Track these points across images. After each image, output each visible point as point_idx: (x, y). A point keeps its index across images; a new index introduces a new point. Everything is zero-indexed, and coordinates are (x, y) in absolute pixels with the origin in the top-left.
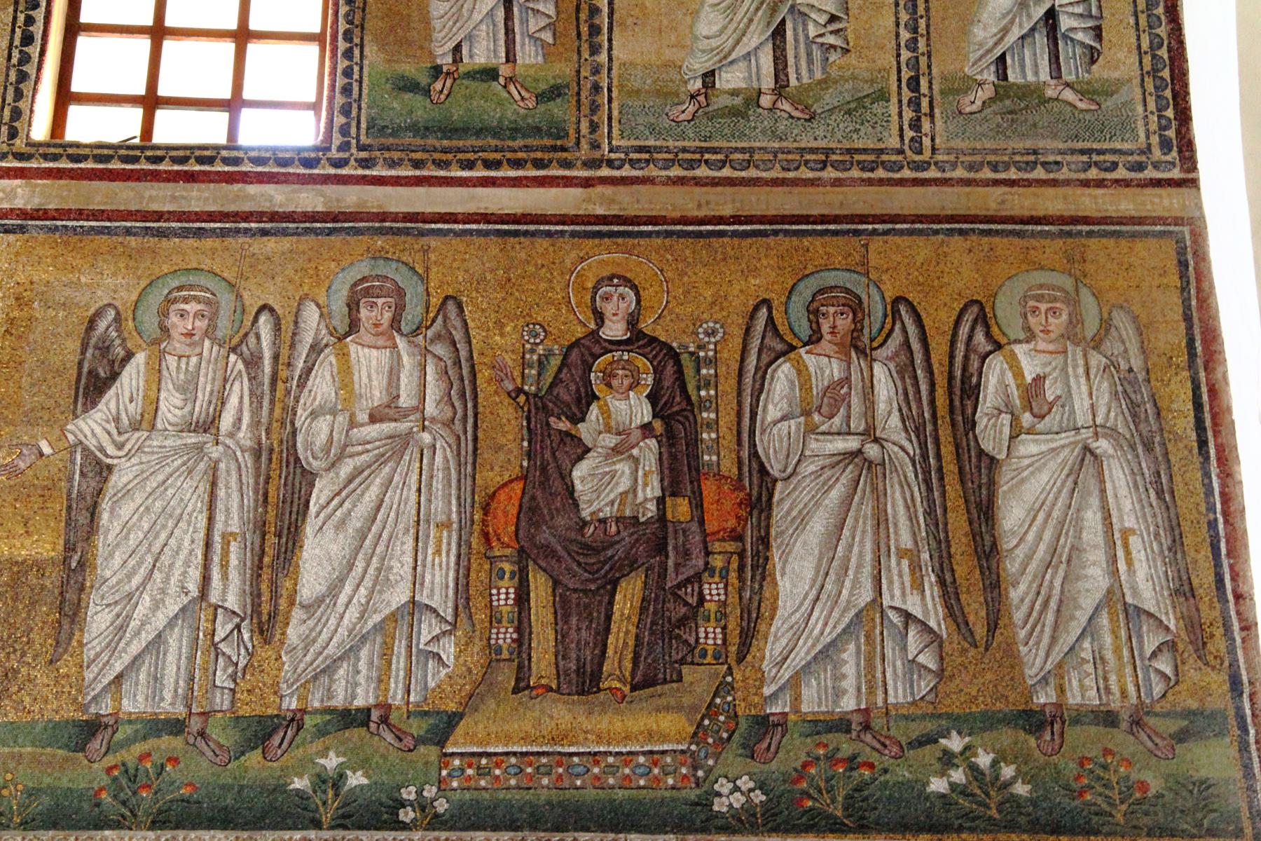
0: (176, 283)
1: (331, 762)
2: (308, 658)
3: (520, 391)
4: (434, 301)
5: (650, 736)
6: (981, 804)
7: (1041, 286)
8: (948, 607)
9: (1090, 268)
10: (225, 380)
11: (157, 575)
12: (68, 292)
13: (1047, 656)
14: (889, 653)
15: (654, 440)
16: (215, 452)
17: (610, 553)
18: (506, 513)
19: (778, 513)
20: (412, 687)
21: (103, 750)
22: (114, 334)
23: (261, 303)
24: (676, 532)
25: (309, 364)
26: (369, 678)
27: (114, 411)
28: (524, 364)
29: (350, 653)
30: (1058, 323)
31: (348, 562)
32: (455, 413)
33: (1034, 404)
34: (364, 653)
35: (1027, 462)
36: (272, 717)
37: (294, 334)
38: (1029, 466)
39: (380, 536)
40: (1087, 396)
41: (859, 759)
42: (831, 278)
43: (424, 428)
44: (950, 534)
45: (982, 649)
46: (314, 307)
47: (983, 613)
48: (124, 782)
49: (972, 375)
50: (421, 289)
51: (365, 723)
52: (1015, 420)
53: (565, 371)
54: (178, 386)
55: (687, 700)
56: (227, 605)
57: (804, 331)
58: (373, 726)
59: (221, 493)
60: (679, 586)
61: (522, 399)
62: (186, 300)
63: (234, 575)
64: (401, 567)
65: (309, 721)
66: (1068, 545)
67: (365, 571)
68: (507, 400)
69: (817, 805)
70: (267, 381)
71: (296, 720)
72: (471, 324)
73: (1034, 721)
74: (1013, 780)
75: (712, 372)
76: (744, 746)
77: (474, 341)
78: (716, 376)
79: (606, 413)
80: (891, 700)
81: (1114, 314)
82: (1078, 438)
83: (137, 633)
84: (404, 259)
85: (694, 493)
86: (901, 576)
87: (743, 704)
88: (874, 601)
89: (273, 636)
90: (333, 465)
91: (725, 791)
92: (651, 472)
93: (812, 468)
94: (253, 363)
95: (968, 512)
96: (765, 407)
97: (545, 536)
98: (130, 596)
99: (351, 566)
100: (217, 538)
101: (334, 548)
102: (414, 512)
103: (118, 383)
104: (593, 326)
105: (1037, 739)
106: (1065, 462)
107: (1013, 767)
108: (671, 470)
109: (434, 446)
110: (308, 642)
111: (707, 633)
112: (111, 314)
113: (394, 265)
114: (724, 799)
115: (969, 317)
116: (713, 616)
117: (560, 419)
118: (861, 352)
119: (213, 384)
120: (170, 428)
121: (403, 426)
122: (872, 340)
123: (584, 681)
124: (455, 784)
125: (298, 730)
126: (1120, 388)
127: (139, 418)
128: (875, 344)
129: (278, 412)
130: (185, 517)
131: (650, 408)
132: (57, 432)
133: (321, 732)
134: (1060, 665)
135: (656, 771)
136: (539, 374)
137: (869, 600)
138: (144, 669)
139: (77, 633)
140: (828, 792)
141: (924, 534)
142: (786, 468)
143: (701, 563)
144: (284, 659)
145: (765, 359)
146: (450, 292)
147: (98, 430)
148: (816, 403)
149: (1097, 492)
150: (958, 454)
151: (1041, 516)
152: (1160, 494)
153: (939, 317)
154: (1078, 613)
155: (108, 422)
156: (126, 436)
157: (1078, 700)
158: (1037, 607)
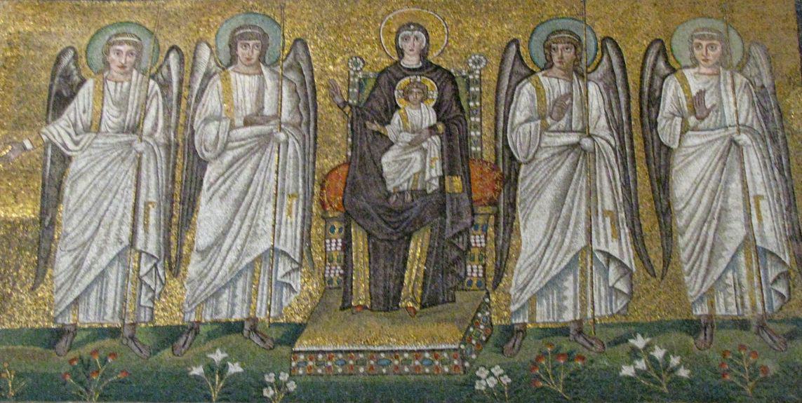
0: (114, 31)
1: (218, 356)
2: (202, 287)
3: (345, 103)
4: (287, 42)
6: (656, 383)
7: (703, 29)
8: (637, 251)
9: (737, 16)
10: (147, 98)
11: (102, 231)
12: (42, 39)
13: (704, 281)
14: (596, 281)
15: (438, 137)
16: (140, 147)
17: (406, 215)
19: (521, 187)
20: (272, 306)
21: (67, 348)
22: (73, 67)
23: (171, 45)
24: (452, 200)
25: (203, 87)
26: (243, 301)
27: (73, 119)
29: (231, 284)
30: (713, 55)
31: (229, 221)
32: (302, 119)
33: (697, 111)
34: (240, 284)
35: (693, 150)
36: (178, 326)
37: (193, 66)
38: (693, 153)
39: (251, 204)
40: (735, 105)
41: (575, 354)
42: (560, 24)
43: (281, 129)
44: (639, 201)
45: (659, 279)
46: (207, 47)
47: (661, 254)
48: (80, 370)
49: (655, 90)
50: (279, 34)
52: (684, 120)
53: (377, 89)
55: (457, 315)
56: (148, 251)
57: (541, 61)
58: (245, 333)
60: (455, 236)
61: (347, 109)
62: (121, 43)
63: (152, 230)
64: (265, 225)
65: (203, 329)
66: (719, 207)
67: (240, 228)
68: (337, 110)
69: (546, 385)
70: (175, 97)
71: (194, 328)
72: (313, 58)
73: (693, 327)
74: (679, 366)
75: (478, 89)
76: (496, 346)
77: (315, 69)
78: (481, 92)
79: (405, 118)
80: (597, 313)
81: (753, 48)
82: (727, 133)
83: (90, 269)
84: (268, 14)
85: (464, 172)
86: (605, 228)
87: (496, 317)
88: (586, 247)
89: (178, 272)
91: (483, 376)
92: (435, 159)
93: (546, 155)
94: (165, 85)
95: (652, 185)
96: (514, 115)
97: (361, 203)
98: (84, 244)
100: (142, 206)
102: (274, 187)
103: (75, 100)
104: (396, 58)
105: (695, 339)
106: (718, 150)
107: (679, 358)
108: (449, 157)
109: (287, 143)
110: (202, 276)
111: (472, 269)
112: (71, 53)
113: (260, 18)
114: (483, 382)
115: (653, 51)
116: (477, 258)
117: (373, 122)
118: (581, 76)
119: (138, 101)
120: (109, 130)
121: (265, 129)
122: (588, 66)
123: (387, 302)
124: (301, 372)
125: (196, 334)
126: (755, 99)
127: (89, 123)
128: (589, 70)
129: (181, 121)
131: (434, 114)
132: (36, 134)
133: (210, 336)
134: (711, 289)
135: (437, 363)
136: (359, 92)
137: (583, 245)
138: (94, 294)
139: (49, 270)
140: (553, 376)
141: (621, 200)
142: (528, 154)
143: (469, 221)
144: (186, 287)
145: (514, 79)
146: (299, 36)
147: (63, 133)
149: (739, 170)
150: (645, 146)
151: (701, 187)
152: (781, 171)
153: (633, 51)
154: (724, 253)
155: (69, 127)
156: (81, 136)
157: (723, 312)
158: (697, 249)
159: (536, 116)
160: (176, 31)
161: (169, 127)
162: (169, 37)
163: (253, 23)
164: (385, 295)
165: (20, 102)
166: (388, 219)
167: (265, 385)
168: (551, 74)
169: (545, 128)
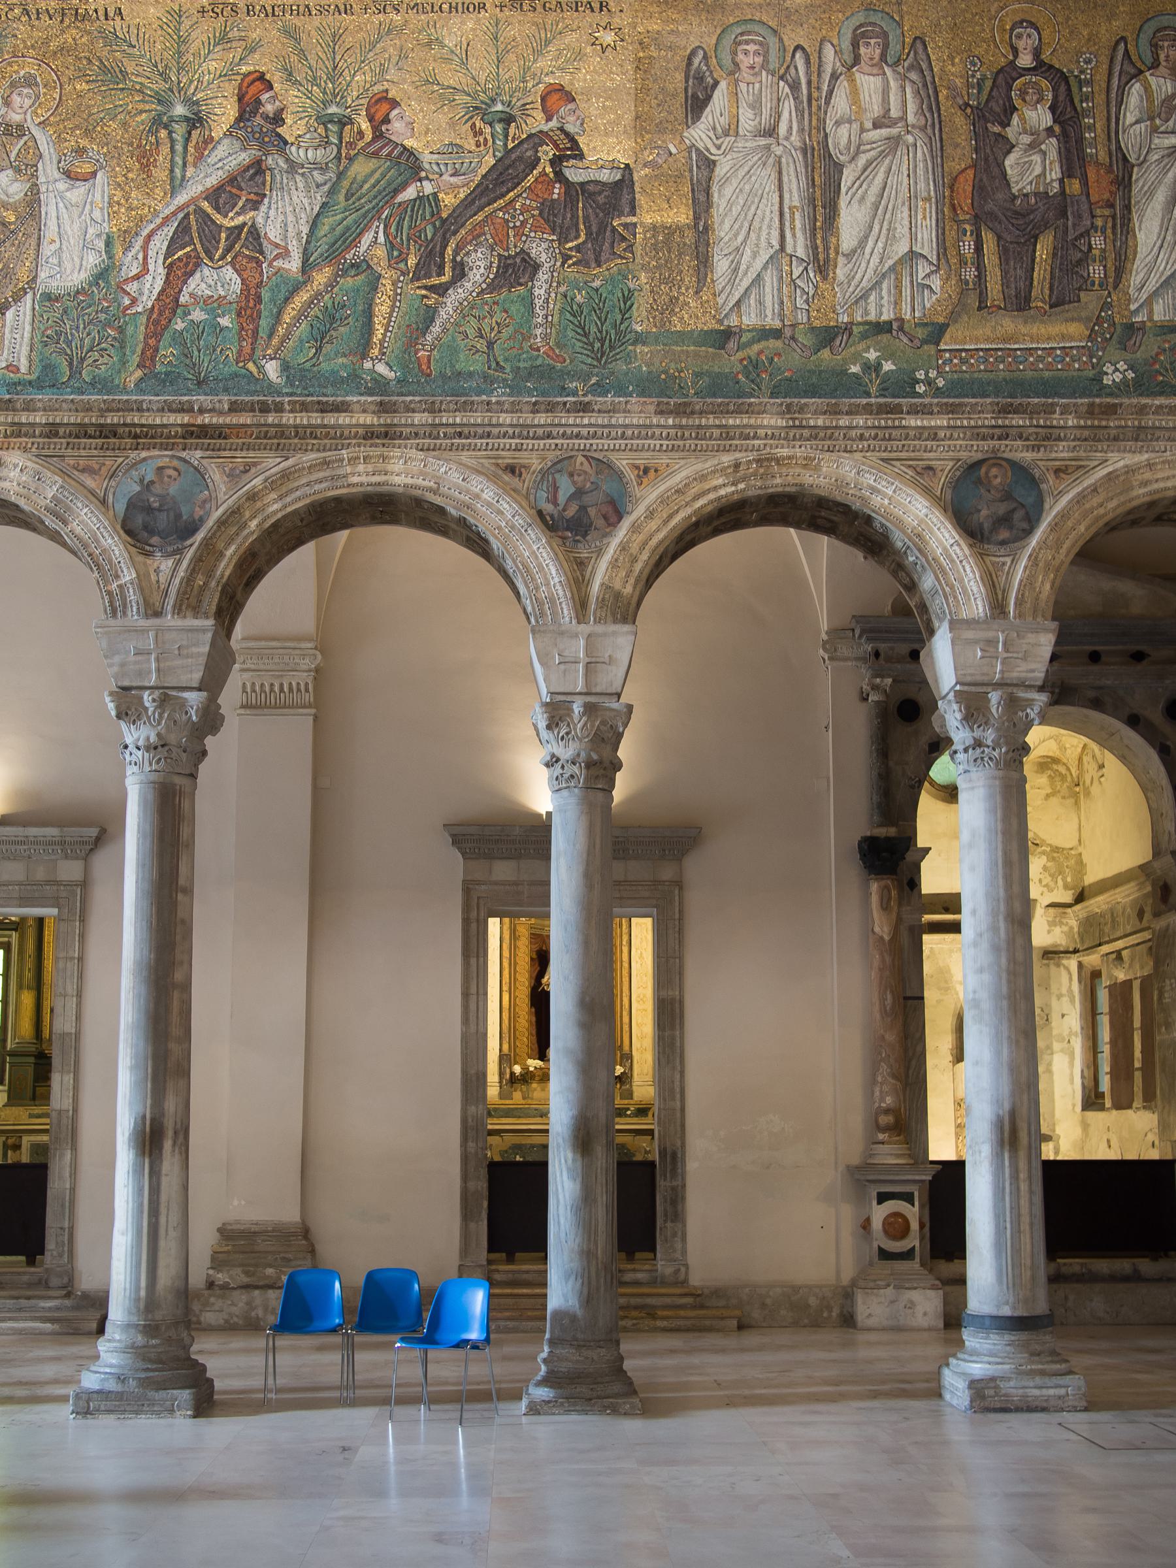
0: (739, 31)
1: (872, 355)
2: (851, 289)
3: (967, 105)
4: (907, 40)
5: (1063, 337)
10: (779, 100)
12: (672, 38)
16: (778, 150)
17: (1032, 217)
18: (964, 191)
19: (1135, 190)
22: (705, 68)
28: (969, 85)
29: (877, 285)
34: (885, 286)
36: (833, 327)
37: (820, 66)
42: (1165, 21)
43: (908, 132)
50: (899, 32)
51: (890, 331)
54: (745, 102)
55: (1083, 314)
57: (1149, 60)
58: (894, 333)
59: (785, 179)
60: (1076, 239)
62: (747, 42)
63: (799, 234)
64: (902, 229)
65: (855, 330)
71: (848, 328)
72: (933, 57)
76: (1120, 343)
79: (1023, 119)
83: (746, 273)
89: (828, 275)
90: (853, 159)
91: (1110, 371)
93: (1156, 157)
94: (795, 86)
97: (990, 206)
98: (738, 249)
99: (871, 228)
100: (786, 210)
101: (859, 215)
104: (1011, 58)
108: (1067, 159)
112: (701, 54)
113: (880, 15)
121: (894, 131)
123: (1020, 302)
124: (947, 369)
129: (814, 123)
130: (765, 195)
136: (979, 93)
138: (753, 296)
143: (1089, 223)
147: (704, 136)
148: (1157, 111)
159: (1145, 117)
160: (799, 30)
161: (803, 130)
162: (793, 36)
163: (872, 20)
164: (1016, 296)
165: (659, 105)
166: (1014, 221)
167: (917, 381)
168: (1158, 73)
169: (1155, 130)
